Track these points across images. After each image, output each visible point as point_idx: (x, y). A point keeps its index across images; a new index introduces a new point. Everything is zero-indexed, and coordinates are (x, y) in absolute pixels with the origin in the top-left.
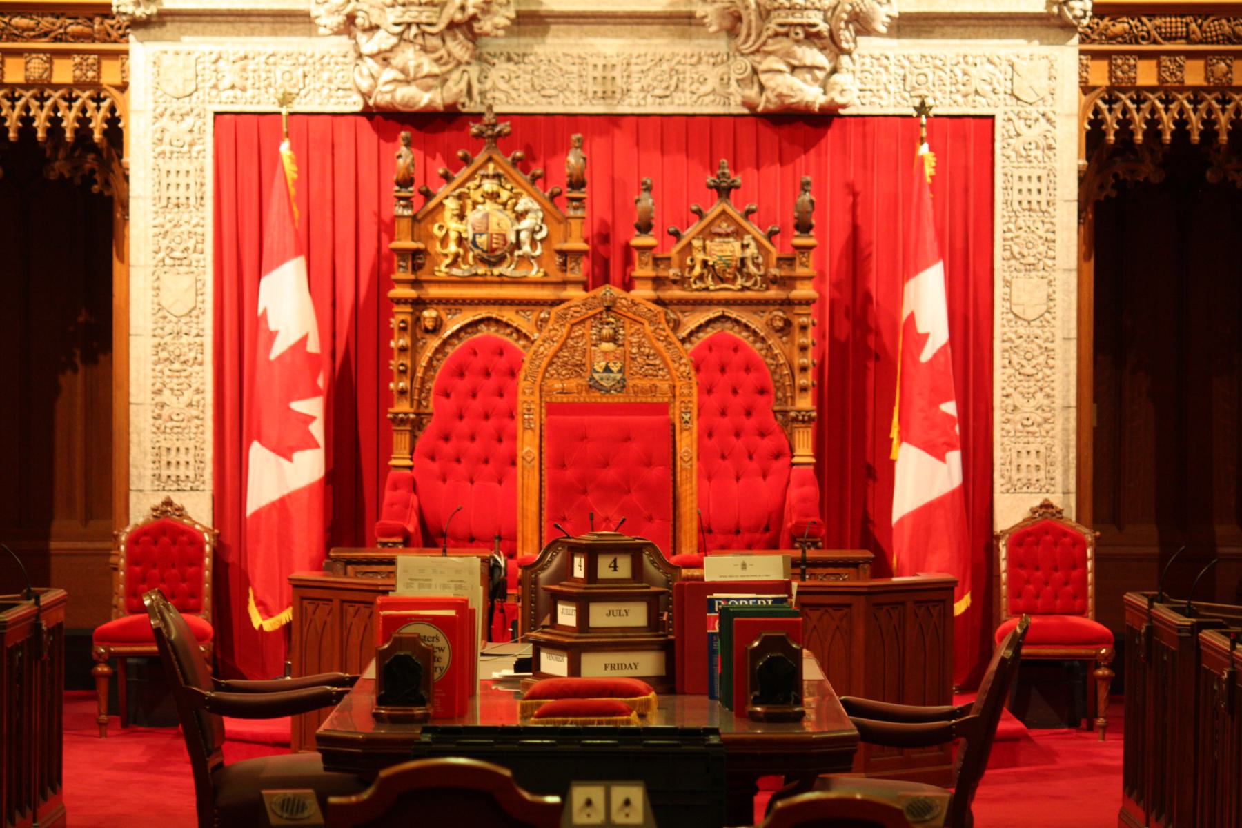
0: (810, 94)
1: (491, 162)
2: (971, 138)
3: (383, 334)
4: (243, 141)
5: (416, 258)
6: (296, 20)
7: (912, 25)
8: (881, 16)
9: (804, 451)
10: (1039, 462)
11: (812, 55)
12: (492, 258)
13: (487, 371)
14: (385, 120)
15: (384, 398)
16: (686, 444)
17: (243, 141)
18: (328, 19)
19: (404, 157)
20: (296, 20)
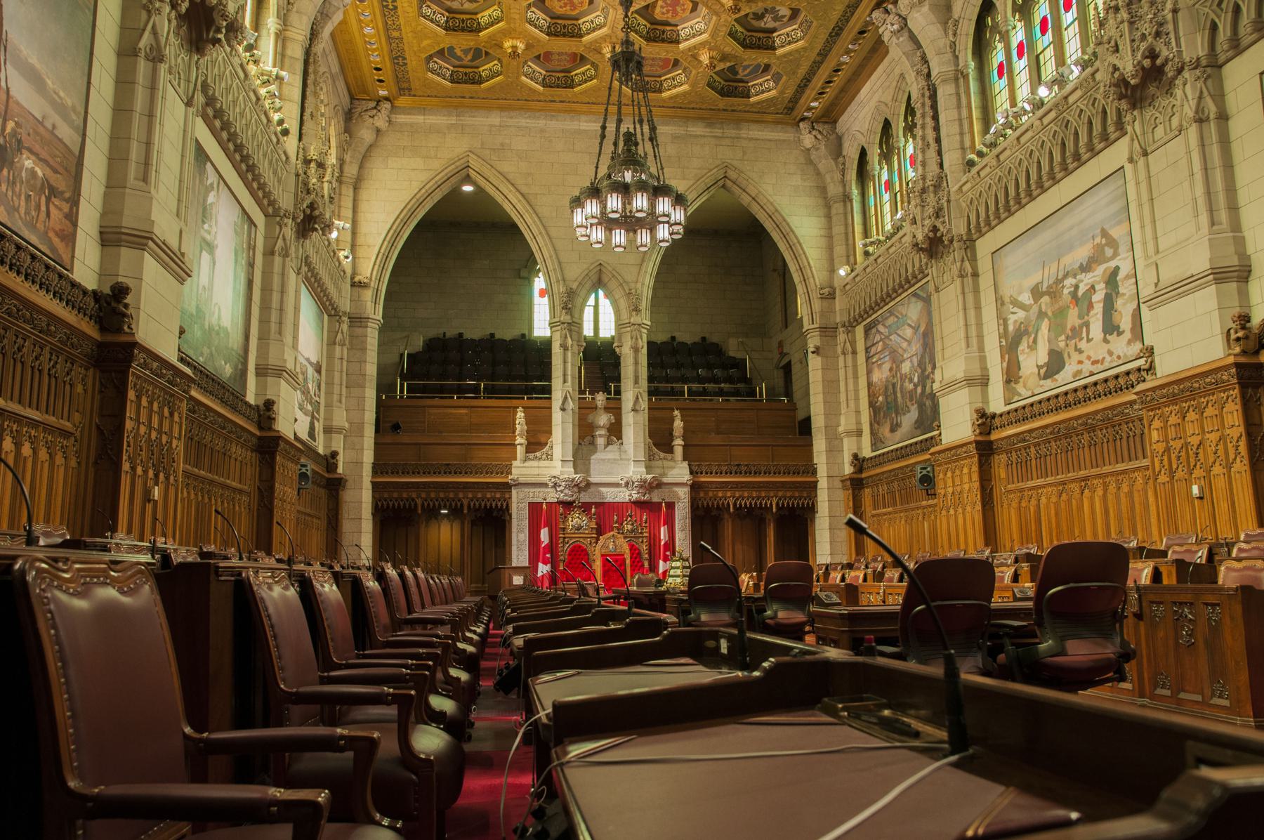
2: (671, 506)
3: (557, 544)
4: (534, 508)
14: (560, 503)
16: (628, 562)
17: (534, 508)
20: (545, 485)
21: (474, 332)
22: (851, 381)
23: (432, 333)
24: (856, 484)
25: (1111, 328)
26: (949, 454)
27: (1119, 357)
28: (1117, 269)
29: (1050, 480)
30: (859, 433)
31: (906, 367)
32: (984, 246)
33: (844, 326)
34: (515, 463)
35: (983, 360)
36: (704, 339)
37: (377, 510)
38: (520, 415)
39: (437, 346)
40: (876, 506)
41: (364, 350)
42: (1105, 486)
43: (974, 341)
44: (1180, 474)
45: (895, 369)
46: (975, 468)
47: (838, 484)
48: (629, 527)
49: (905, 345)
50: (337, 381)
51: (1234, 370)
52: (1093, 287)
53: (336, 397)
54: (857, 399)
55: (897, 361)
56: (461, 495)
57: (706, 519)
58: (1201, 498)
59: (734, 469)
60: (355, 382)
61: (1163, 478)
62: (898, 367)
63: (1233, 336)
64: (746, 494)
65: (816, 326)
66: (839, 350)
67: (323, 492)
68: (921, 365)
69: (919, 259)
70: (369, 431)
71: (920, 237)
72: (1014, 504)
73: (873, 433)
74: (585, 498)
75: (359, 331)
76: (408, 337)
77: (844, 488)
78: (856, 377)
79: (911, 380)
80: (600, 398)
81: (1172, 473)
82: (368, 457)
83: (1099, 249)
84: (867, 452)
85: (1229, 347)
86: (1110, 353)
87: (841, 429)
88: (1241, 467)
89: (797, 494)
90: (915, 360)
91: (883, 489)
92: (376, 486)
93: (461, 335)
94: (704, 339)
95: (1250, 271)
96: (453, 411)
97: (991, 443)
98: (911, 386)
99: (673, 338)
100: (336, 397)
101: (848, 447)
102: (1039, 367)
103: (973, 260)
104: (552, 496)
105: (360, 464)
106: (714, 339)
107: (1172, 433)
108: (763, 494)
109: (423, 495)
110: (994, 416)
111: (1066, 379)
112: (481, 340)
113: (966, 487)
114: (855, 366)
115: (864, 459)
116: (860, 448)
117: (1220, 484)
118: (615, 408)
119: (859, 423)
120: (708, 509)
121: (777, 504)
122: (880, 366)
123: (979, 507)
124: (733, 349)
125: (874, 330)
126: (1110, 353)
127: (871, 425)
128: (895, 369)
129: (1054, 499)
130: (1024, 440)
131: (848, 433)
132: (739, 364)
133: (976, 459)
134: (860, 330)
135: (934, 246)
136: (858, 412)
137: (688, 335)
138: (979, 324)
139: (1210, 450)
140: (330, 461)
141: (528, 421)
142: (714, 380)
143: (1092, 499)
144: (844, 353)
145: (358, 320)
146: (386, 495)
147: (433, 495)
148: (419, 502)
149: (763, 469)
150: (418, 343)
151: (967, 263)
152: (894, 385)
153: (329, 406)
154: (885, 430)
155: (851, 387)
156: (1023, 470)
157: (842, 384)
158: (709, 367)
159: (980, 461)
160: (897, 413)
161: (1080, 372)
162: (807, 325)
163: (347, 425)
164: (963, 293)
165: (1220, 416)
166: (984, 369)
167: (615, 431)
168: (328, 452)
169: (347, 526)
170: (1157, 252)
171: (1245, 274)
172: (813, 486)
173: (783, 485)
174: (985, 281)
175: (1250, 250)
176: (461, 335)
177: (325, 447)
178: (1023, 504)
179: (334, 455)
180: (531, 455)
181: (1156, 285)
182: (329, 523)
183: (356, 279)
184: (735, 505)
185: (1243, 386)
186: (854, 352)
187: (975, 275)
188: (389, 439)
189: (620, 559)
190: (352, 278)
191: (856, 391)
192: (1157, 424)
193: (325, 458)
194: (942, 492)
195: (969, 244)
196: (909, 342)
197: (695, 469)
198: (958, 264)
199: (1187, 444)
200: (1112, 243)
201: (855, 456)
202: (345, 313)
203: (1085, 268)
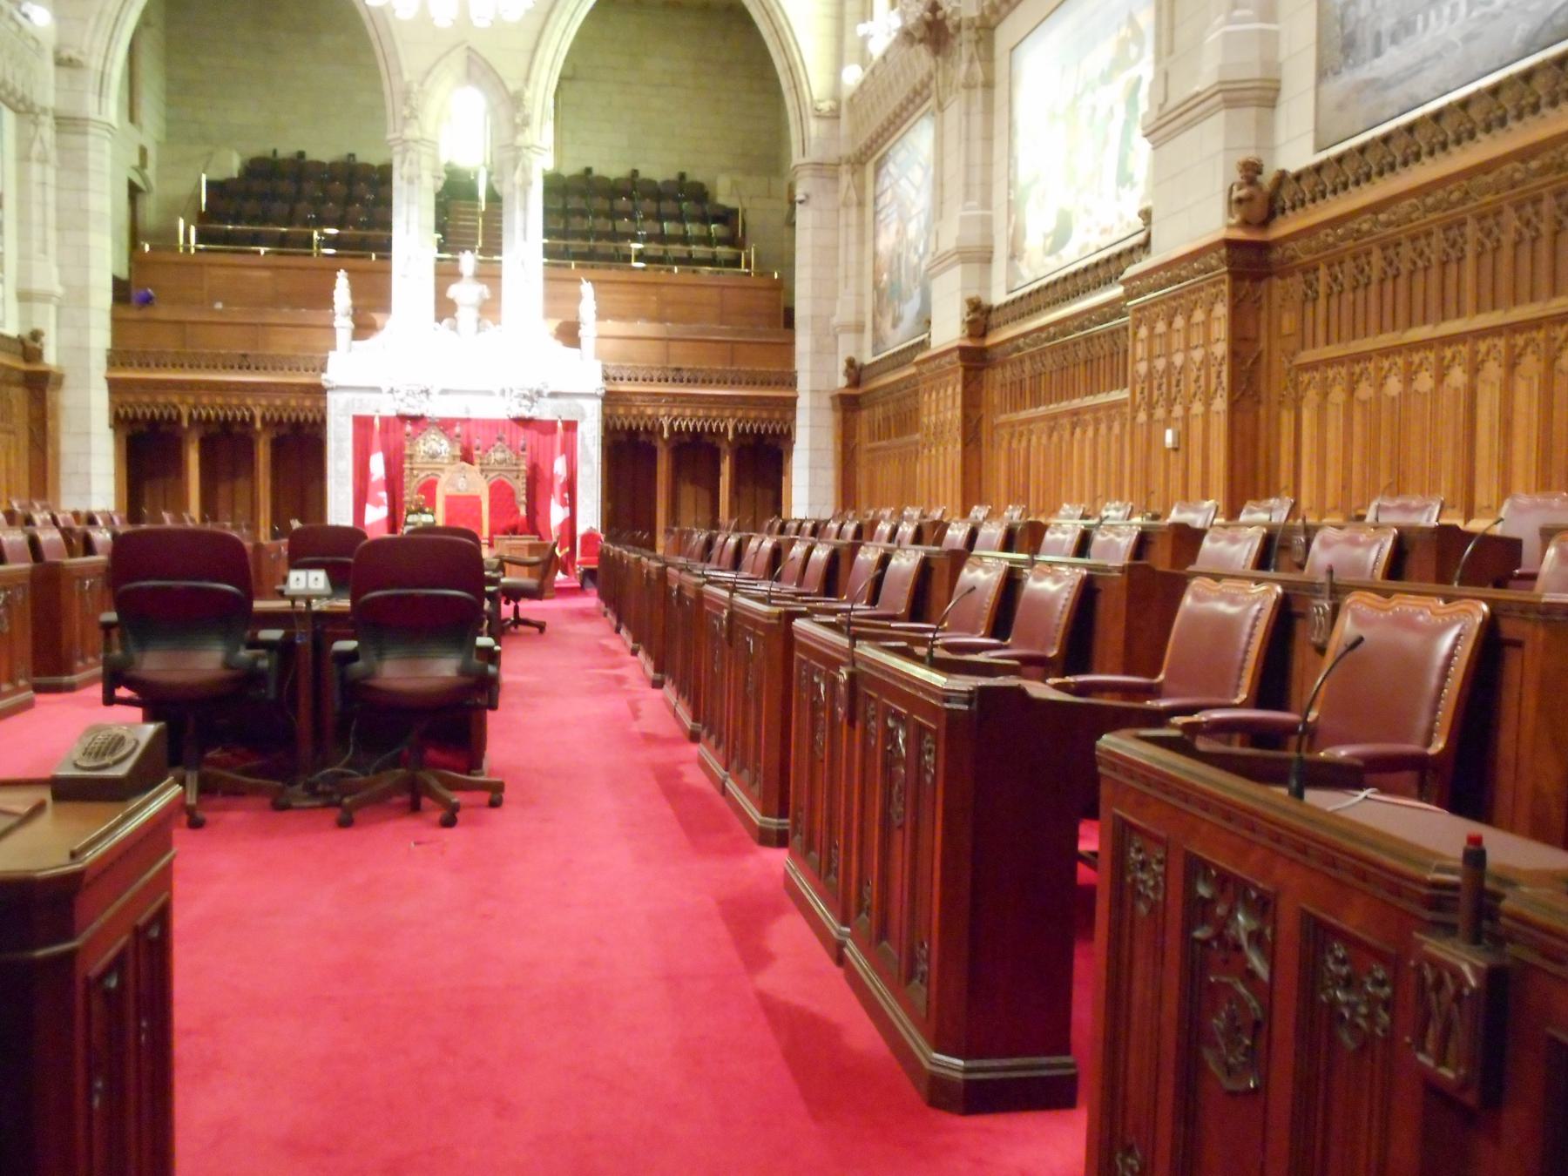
0: (527, 414)
1: (433, 430)
2: (571, 426)
4: (362, 424)
5: (411, 456)
6: (377, 390)
7: (554, 395)
8: (546, 392)
9: (523, 511)
10: (590, 518)
11: (526, 402)
12: (433, 456)
13: (429, 488)
14: (403, 418)
15: (402, 496)
17: (362, 424)
18: (385, 389)
19: (409, 428)
20: (377, 390)
21: (324, 149)
22: (853, 249)
23: (260, 148)
24: (849, 405)
25: (1124, 179)
26: (933, 365)
27: (1129, 225)
28: (1140, 79)
29: (1042, 410)
30: (859, 328)
31: (913, 229)
32: (1004, 36)
33: (848, 162)
34: (334, 359)
35: (987, 222)
36: (682, 176)
37: (119, 421)
38: (342, 284)
39: (262, 171)
40: (872, 436)
41: (83, 170)
42: (1097, 421)
43: (977, 192)
44: (1160, 413)
45: (901, 232)
46: (959, 388)
47: (827, 403)
48: (499, 456)
49: (913, 193)
50: (36, 215)
51: (1223, 252)
52: (1111, 110)
53: (36, 245)
54: (860, 274)
55: (904, 221)
56: (249, 401)
57: (627, 450)
58: (1176, 450)
59: (671, 375)
60: (72, 221)
61: (1142, 417)
62: (905, 229)
63: (1237, 194)
64: (688, 412)
65: (808, 159)
66: (841, 197)
67: (18, 395)
68: (928, 228)
69: (922, 58)
70: (102, 298)
71: (911, 21)
72: (1005, 444)
73: (875, 329)
74: (436, 408)
75: (74, 140)
76: (211, 154)
77: (834, 408)
78: (861, 241)
79: (916, 249)
80: (468, 261)
81: (1151, 407)
82: (100, 338)
83: (1123, 44)
84: (868, 358)
85: (1231, 214)
86: (1121, 218)
87: (835, 321)
88: (1220, 404)
89: (765, 415)
90: (922, 217)
91: (879, 412)
92: (114, 386)
93: (301, 155)
94: (682, 176)
95: (1278, 90)
96: (248, 273)
97: (983, 351)
98: (914, 259)
99: (635, 173)
100: (36, 245)
101: (846, 348)
102: (1046, 236)
103: (989, 58)
104: (384, 407)
105: (83, 349)
106: (697, 175)
107: (1157, 350)
108: (714, 413)
109: (191, 400)
110: (990, 310)
111: (1073, 257)
112: (333, 165)
113: (949, 415)
114: (861, 224)
115: (862, 368)
116: (859, 350)
117: (1197, 428)
118: (489, 275)
119: (860, 312)
120: (632, 433)
121: (735, 429)
122: (887, 226)
123: (959, 447)
124: (724, 196)
125: (883, 171)
126: (1121, 218)
127: (874, 317)
128: (901, 232)
129: (1044, 440)
130: (1018, 349)
131: (845, 328)
132: (727, 217)
133: (961, 372)
134: (870, 168)
135: (934, 32)
136: (860, 295)
137: (657, 170)
138: (988, 165)
139: (1193, 375)
140: (29, 347)
141: (355, 293)
142: (684, 240)
143: (1082, 441)
144: (846, 205)
145: (69, 124)
146: (131, 399)
147: (205, 400)
148: (184, 411)
149: (715, 377)
150: (231, 165)
151: (978, 68)
152: (899, 256)
153: (24, 257)
154: (886, 324)
155: (853, 257)
156: (1021, 394)
157: (841, 251)
158: (679, 218)
159: (965, 378)
160: (900, 300)
161: (1086, 246)
162: (796, 158)
163: (59, 290)
164: (968, 114)
165: (1207, 325)
166: (988, 236)
167: (489, 309)
168: (26, 333)
169: (67, 444)
170: (1171, 52)
171: (1271, 94)
172: (791, 404)
173: (745, 400)
174: (1000, 92)
175: (1283, 54)
176: (301, 155)
177: (22, 322)
178: (1014, 445)
179: (36, 336)
180: (357, 344)
181: (1161, 106)
182: (32, 440)
183: (65, 54)
184: (671, 426)
185: (1236, 276)
186: (861, 204)
187: (989, 85)
188: (132, 313)
189: (474, 501)
190: (57, 52)
191: (861, 263)
192: (1143, 332)
193: (20, 340)
194: (925, 420)
195: (985, 30)
196: (918, 190)
197: (612, 373)
198: (964, 67)
199: (1170, 365)
200: (1138, 36)
201: (851, 363)
202: (44, 111)
203: (1106, 78)
